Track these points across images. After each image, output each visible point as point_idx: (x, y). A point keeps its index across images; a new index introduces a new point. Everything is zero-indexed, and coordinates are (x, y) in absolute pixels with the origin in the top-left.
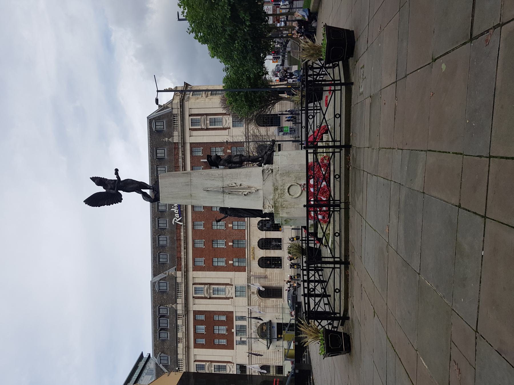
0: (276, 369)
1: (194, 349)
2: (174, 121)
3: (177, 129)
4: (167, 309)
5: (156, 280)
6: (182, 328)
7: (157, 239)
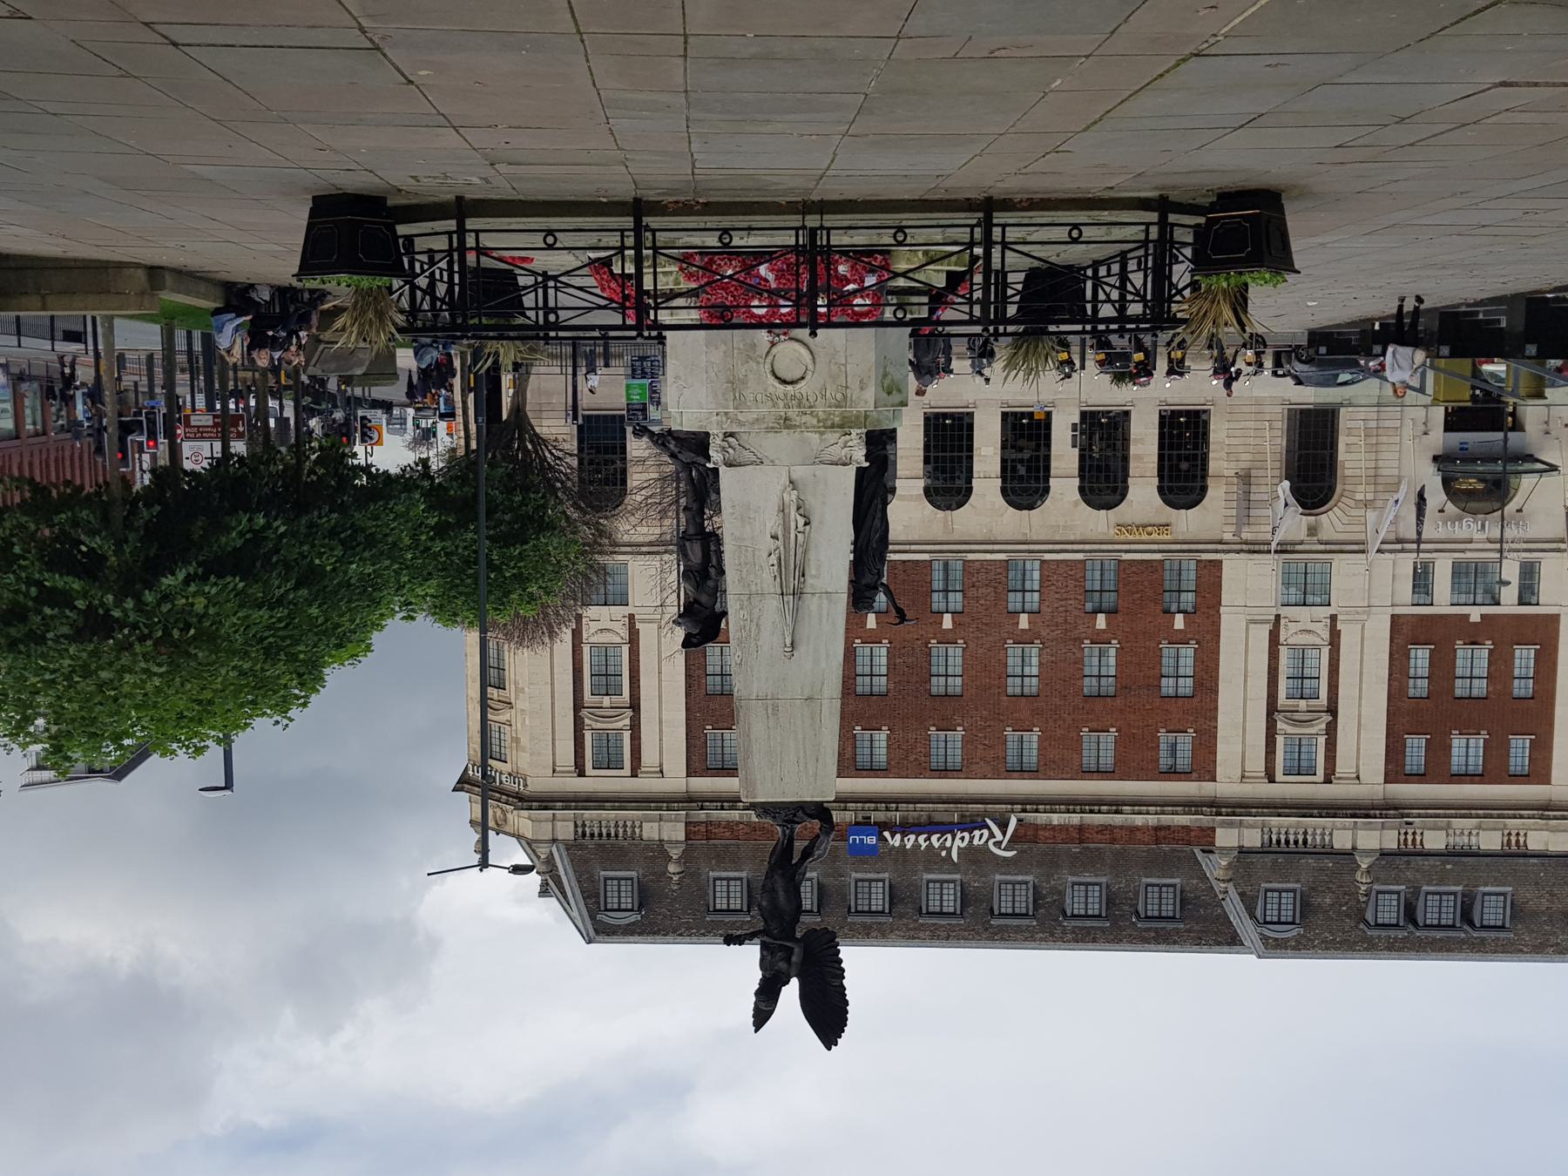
1: (1553, 782)
2: (600, 835)
3: (633, 827)
4: (1379, 892)
5: (1256, 937)
6: (1462, 833)
7: (1079, 923)
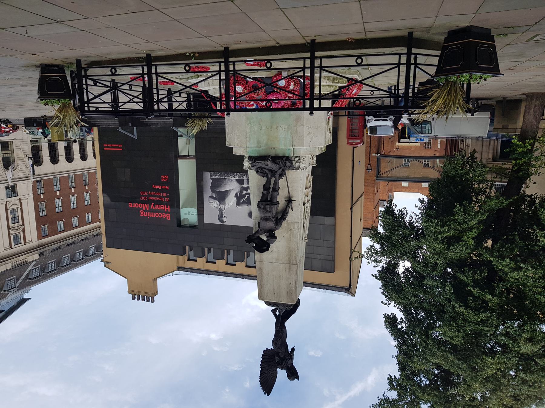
0: (4, 150)
